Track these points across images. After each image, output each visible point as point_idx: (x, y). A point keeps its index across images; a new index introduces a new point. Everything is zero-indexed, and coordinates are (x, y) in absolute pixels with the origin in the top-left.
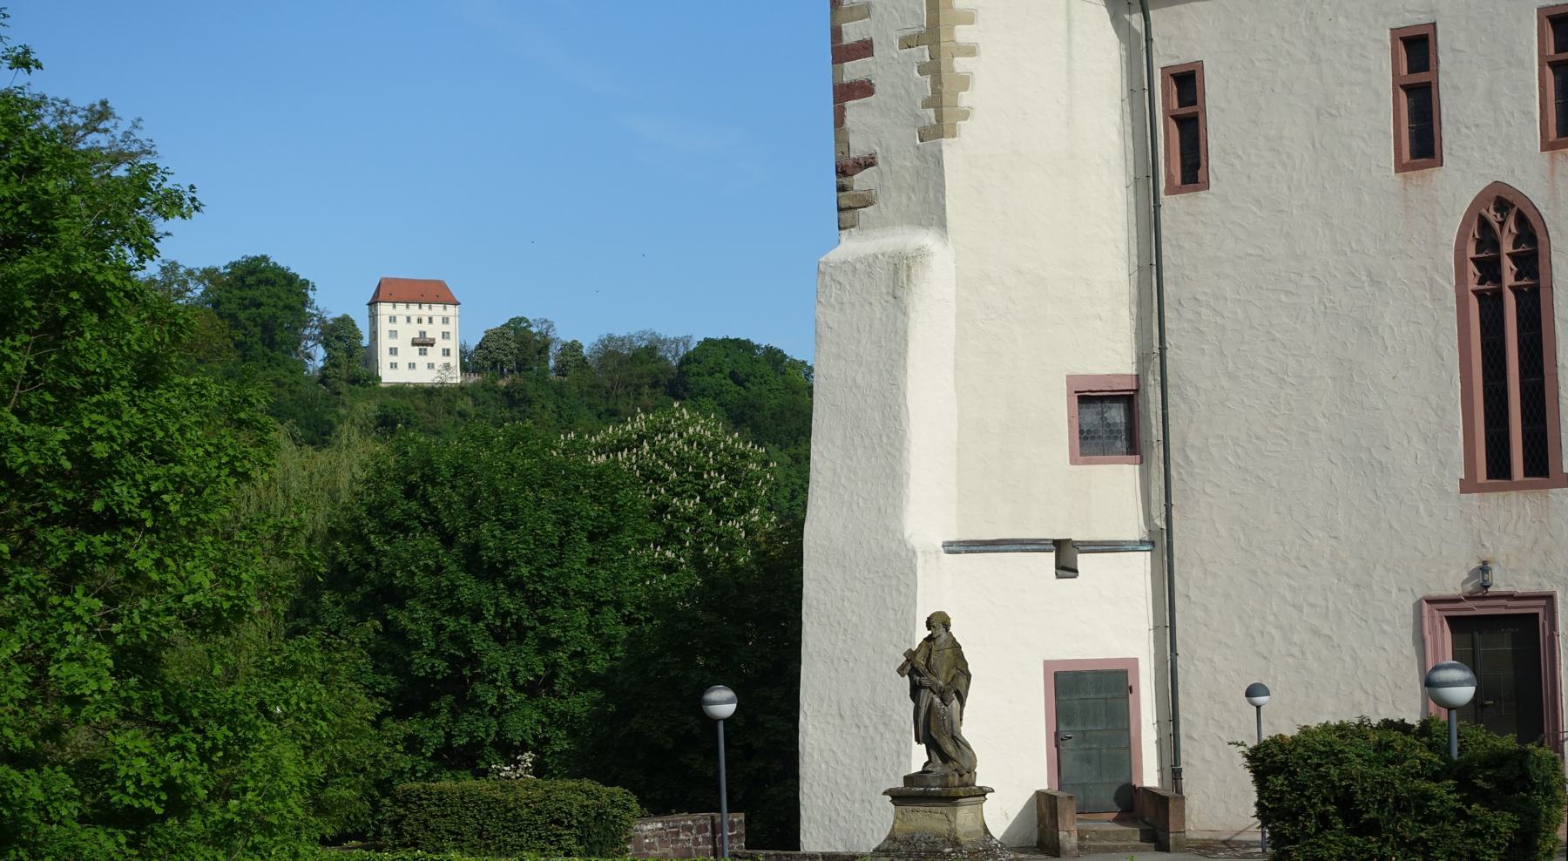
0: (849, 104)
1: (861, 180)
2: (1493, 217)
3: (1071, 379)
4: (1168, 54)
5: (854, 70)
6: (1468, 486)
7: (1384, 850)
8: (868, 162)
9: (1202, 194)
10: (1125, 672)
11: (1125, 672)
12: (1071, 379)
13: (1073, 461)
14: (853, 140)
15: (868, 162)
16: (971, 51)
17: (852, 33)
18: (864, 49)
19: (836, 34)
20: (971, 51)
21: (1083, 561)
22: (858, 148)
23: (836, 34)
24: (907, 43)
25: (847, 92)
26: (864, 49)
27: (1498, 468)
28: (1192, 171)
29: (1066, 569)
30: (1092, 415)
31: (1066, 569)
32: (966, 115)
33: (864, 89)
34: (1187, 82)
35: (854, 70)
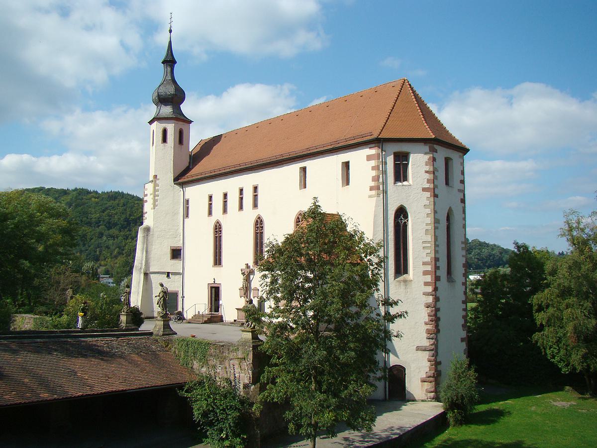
4: (186, 198)
28: (187, 216)
29: (168, 276)
31: (168, 276)
34: (188, 201)
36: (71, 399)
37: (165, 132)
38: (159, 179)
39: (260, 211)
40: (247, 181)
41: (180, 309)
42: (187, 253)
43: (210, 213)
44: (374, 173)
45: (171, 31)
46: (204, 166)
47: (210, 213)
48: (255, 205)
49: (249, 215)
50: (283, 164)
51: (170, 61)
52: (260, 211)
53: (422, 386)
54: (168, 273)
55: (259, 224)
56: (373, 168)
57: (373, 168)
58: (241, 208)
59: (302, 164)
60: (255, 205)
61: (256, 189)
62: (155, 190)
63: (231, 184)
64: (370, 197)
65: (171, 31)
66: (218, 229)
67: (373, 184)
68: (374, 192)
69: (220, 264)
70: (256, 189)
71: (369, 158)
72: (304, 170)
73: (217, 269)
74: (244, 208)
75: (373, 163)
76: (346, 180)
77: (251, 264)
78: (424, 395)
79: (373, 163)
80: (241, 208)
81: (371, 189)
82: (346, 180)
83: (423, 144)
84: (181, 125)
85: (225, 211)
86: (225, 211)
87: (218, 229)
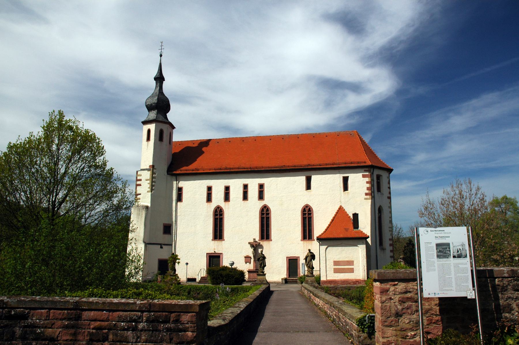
0: (138, 187)
1: (138, 197)
3: (164, 224)
5: (138, 183)
6: (212, 240)
8: (140, 194)
9: (182, 203)
12: (164, 224)
14: (138, 191)
15: (140, 194)
17: (139, 178)
18: (140, 180)
19: (137, 178)
21: (164, 247)
22: (138, 192)
23: (137, 178)
24: (147, 180)
25: (137, 185)
26: (140, 180)
29: (161, 247)
31: (161, 247)
33: (140, 185)
35: (138, 183)
43: (209, 199)
44: (368, 185)
45: (161, 56)
46: (199, 164)
47: (209, 199)
48: (261, 196)
51: (160, 79)
52: (267, 201)
54: (160, 244)
56: (367, 182)
57: (367, 182)
59: (308, 173)
60: (261, 196)
64: (366, 199)
65: (161, 56)
67: (367, 192)
68: (368, 197)
71: (364, 176)
73: (217, 243)
75: (367, 179)
76: (346, 188)
77: (257, 239)
79: (367, 179)
81: (366, 194)
82: (346, 188)
83: (386, 172)
84: (165, 127)
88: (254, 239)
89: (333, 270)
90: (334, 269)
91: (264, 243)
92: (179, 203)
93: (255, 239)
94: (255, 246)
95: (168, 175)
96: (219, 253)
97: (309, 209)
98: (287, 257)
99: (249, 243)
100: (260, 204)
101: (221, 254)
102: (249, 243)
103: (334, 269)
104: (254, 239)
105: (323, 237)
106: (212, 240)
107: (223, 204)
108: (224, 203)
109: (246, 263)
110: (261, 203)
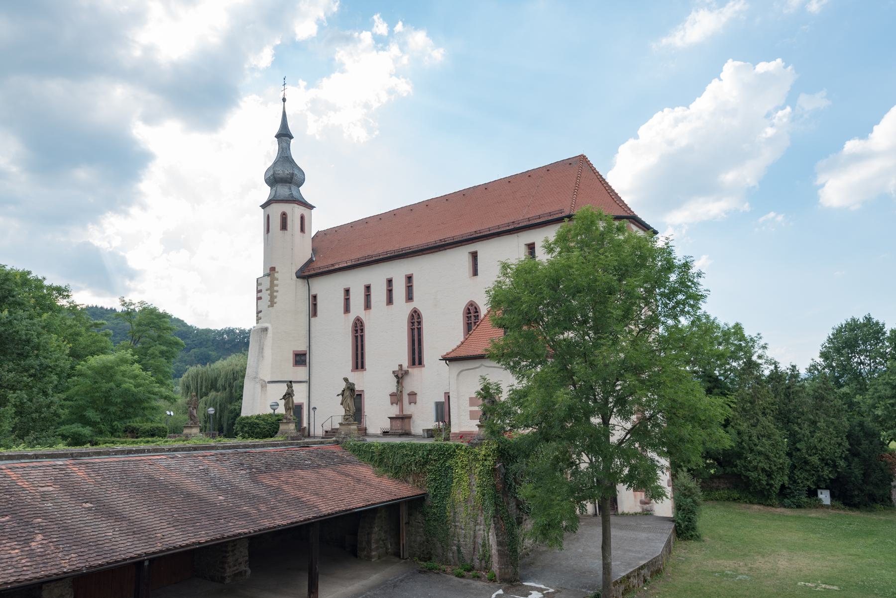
1: (260, 315)
2: (357, 322)
3: (293, 351)
4: (313, 292)
5: (260, 295)
6: (352, 371)
7: (138, 421)
10: (301, 406)
11: (301, 406)
12: (293, 351)
13: (293, 366)
15: (261, 312)
16: (277, 291)
20: (277, 291)
24: (267, 290)
27: (357, 368)
28: (315, 314)
30: (298, 358)
32: (276, 303)
34: (315, 297)
36: (189, 548)
37: (284, 217)
38: (277, 272)
39: (415, 304)
40: (398, 271)
41: (305, 424)
42: (316, 358)
49: (402, 309)
50: (446, 249)
51: (284, 135)
52: (415, 304)
53: (635, 496)
55: (415, 321)
58: (390, 301)
59: (472, 248)
61: (409, 278)
62: (272, 285)
63: (376, 277)
66: (358, 328)
69: (363, 367)
70: (409, 278)
72: (474, 255)
74: (394, 301)
77: (405, 365)
78: (639, 508)
80: (390, 301)
85: (368, 306)
86: (368, 306)
87: (358, 328)
88: (399, 366)
89: (469, 413)
90: (470, 411)
91: (415, 371)
92: (313, 319)
93: (401, 366)
94: (400, 376)
95: (298, 279)
96: (360, 390)
97: (476, 308)
98: (445, 393)
99: (394, 372)
100: (408, 308)
101: (363, 391)
102: (394, 372)
103: (470, 411)
104: (399, 366)
105: (449, 356)
106: (352, 371)
107: (362, 314)
108: (364, 312)
109: (392, 404)
110: (411, 306)
